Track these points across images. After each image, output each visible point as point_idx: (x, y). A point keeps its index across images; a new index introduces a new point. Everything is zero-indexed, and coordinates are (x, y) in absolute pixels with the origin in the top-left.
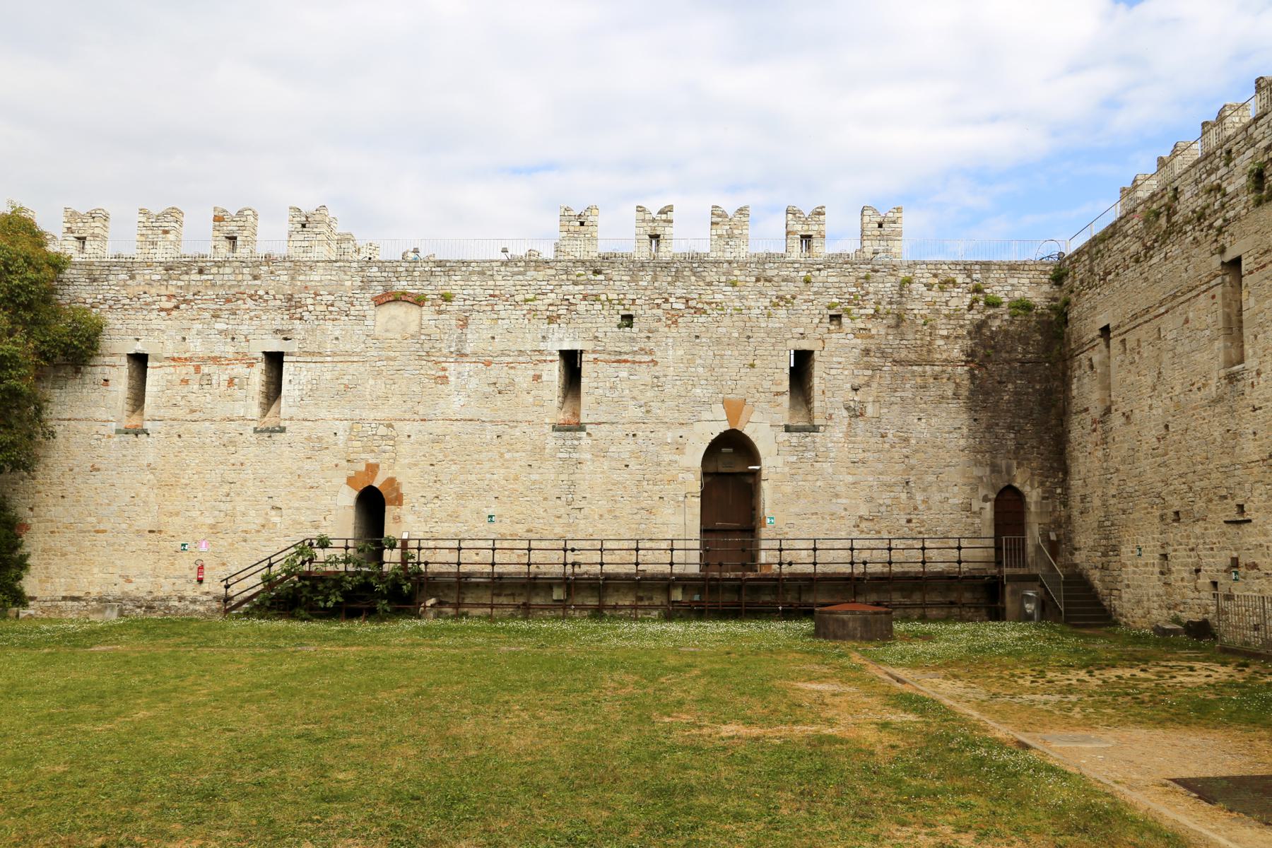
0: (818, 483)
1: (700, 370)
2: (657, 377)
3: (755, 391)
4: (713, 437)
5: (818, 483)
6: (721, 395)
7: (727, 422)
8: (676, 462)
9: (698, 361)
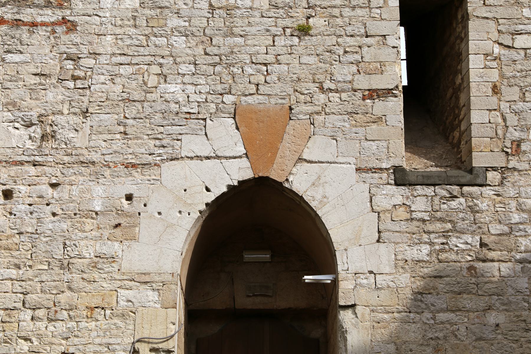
0: (492, 318)
1: (179, 42)
2: (75, 59)
3: (313, 88)
4: (211, 197)
5: (492, 318)
6: (229, 99)
7: (245, 162)
8: (113, 259)
9: (174, 22)
